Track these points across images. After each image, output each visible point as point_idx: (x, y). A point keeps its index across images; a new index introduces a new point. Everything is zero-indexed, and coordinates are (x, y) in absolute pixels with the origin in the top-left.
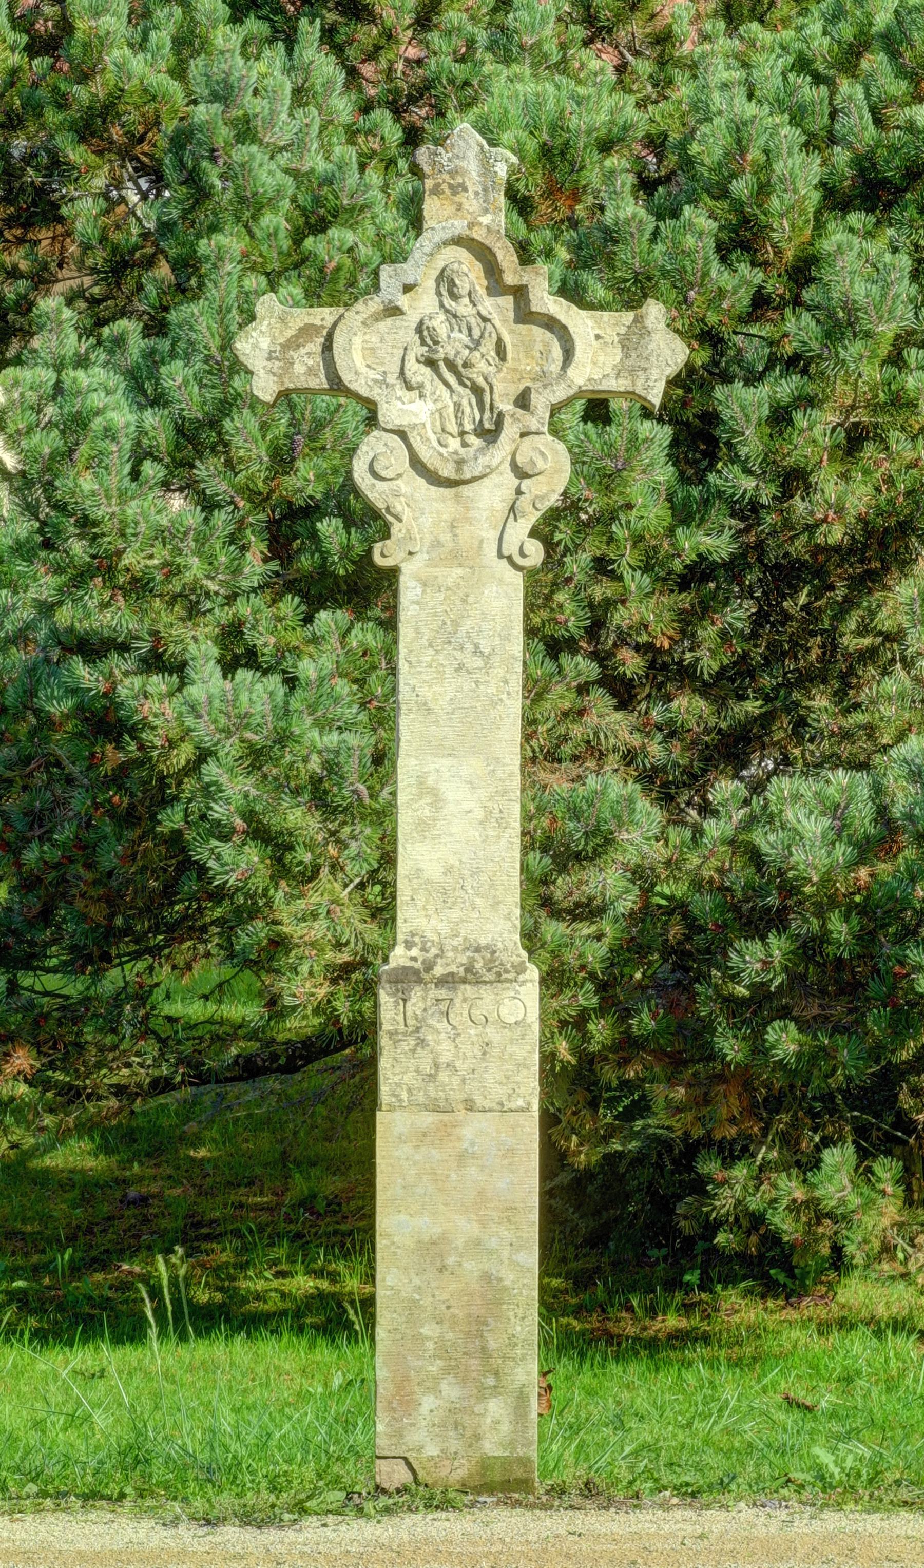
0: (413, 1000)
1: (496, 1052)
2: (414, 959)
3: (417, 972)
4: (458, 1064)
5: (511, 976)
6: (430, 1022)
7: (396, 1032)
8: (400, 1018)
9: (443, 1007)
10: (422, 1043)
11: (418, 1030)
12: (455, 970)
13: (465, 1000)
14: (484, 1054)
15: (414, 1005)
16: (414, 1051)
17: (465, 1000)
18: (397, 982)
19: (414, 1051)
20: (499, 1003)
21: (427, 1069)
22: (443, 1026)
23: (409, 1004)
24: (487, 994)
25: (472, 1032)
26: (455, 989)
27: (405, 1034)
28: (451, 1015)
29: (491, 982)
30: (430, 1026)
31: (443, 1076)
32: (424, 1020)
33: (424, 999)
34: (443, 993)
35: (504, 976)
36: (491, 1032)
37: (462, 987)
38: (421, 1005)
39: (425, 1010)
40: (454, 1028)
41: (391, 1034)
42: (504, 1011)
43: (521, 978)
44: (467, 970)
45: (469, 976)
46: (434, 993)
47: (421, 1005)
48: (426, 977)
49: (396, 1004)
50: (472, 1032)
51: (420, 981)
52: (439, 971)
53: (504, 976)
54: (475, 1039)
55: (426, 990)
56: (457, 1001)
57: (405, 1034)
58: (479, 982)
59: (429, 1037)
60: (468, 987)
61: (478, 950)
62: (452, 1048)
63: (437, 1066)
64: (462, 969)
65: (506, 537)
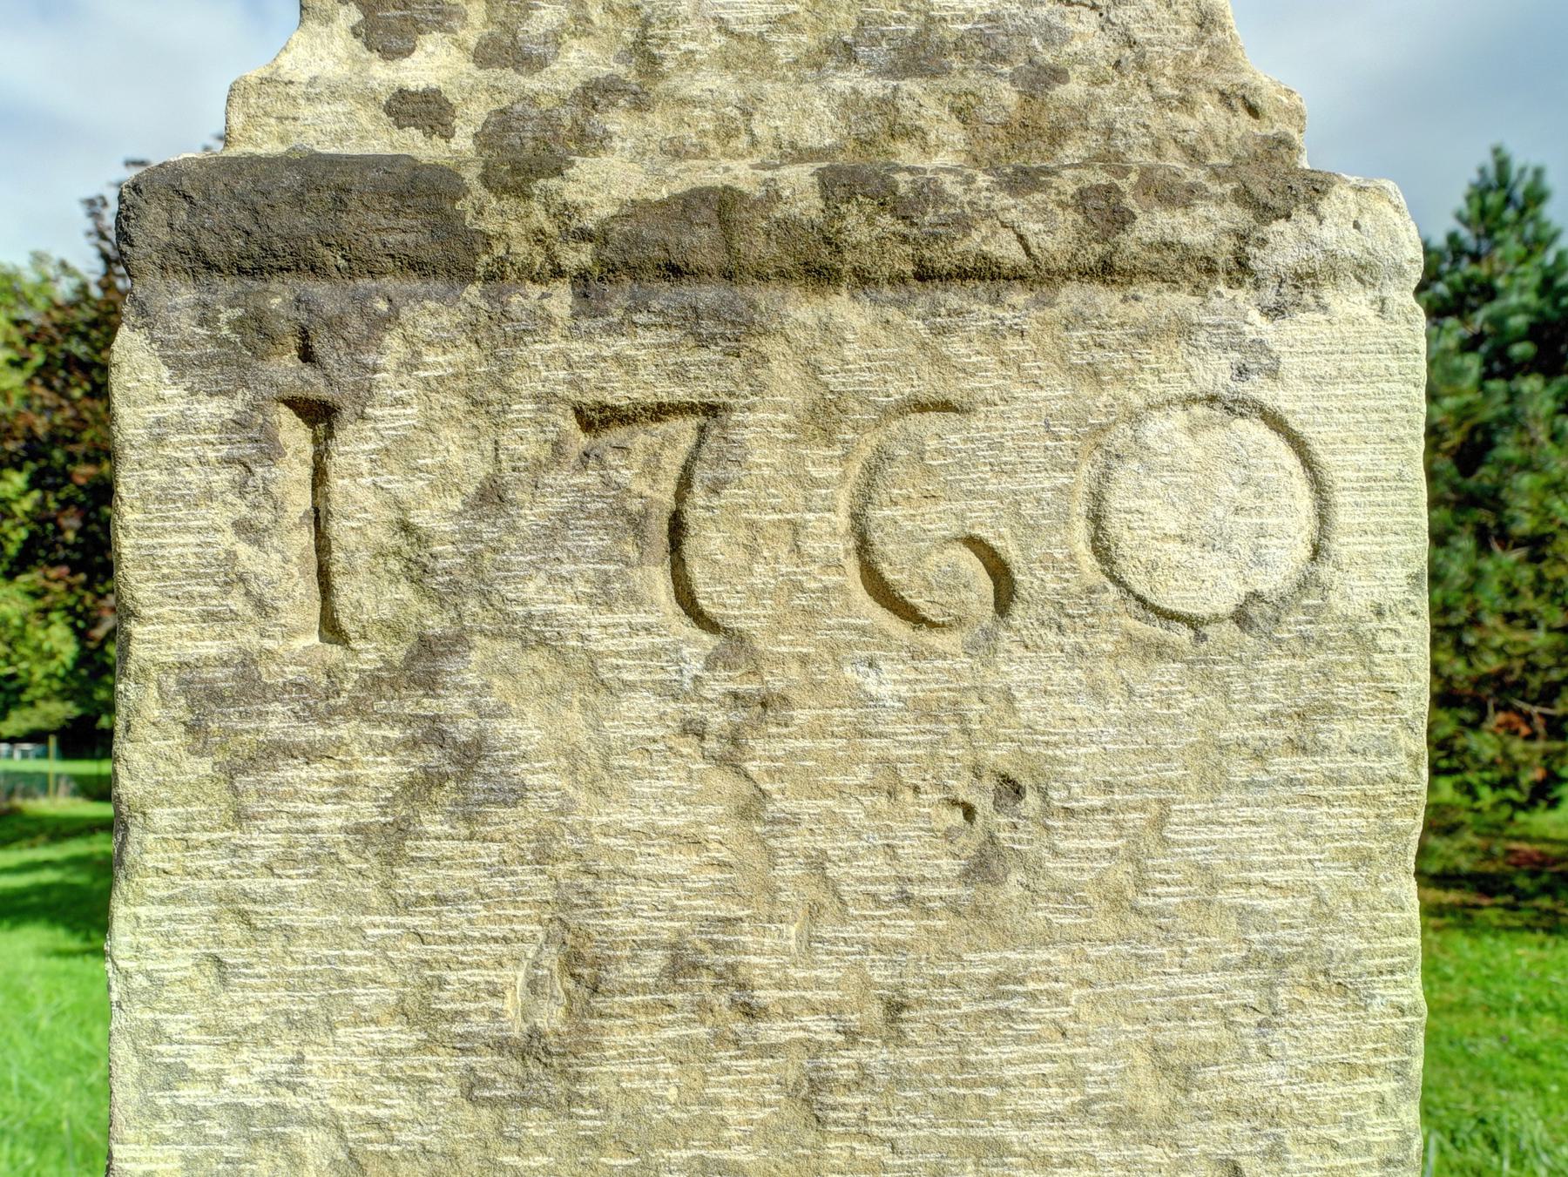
0: (393, 416)
1: (1083, 853)
2: (423, 110)
3: (422, 190)
4: (764, 953)
5: (1203, 226)
6: (532, 593)
7: (248, 683)
8: (283, 564)
9: (643, 468)
10: (460, 770)
11: (426, 660)
12: (742, 174)
13: (823, 418)
14: (983, 867)
15: (398, 451)
16: (390, 840)
17: (823, 418)
18: (256, 266)
19: (390, 840)
20: (1104, 446)
21: (507, 988)
22: (638, 625)
23: (353, 447)
24: (1014, 372)
25: (887, 683)
26: (738, 331)
27: (318, 699)
28: (711, 543)
29: (1037, 276)
30: (535, 634)
31: (639, 1058)
32: (478, 574)
33: (484, 404)
34: (636, 359)
35: (1154, 223)
36: (1056, 697)
37: (802, 310)
38: (459, 454)
39: (491, 496)
40: (734, 645)
41: (206, 699)
42: (1148, 516)
43: (1284, 245)
44: (839, 184)
45: (858, 226)
46: (565, 354)
47: (459, 454)
48: (505, 223)
49: (251, 445)
50: (887, 683)
51: (451, 257)
52: (610, 179)
53: (1154, 223)
54: (904, 740)
55: (501, 336)
56: (761, 429)
57: (318, 699)
58: (938, 275)
59: (524, 727)
60: (845, 309)
61: (919, 56)
62: (713, 817)
63: (585, 969)
64: (798, 179)
65: (1115, 525)
